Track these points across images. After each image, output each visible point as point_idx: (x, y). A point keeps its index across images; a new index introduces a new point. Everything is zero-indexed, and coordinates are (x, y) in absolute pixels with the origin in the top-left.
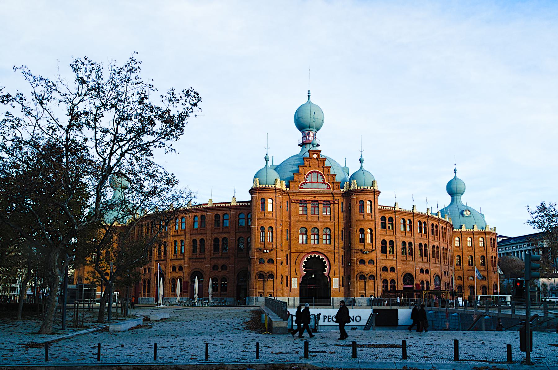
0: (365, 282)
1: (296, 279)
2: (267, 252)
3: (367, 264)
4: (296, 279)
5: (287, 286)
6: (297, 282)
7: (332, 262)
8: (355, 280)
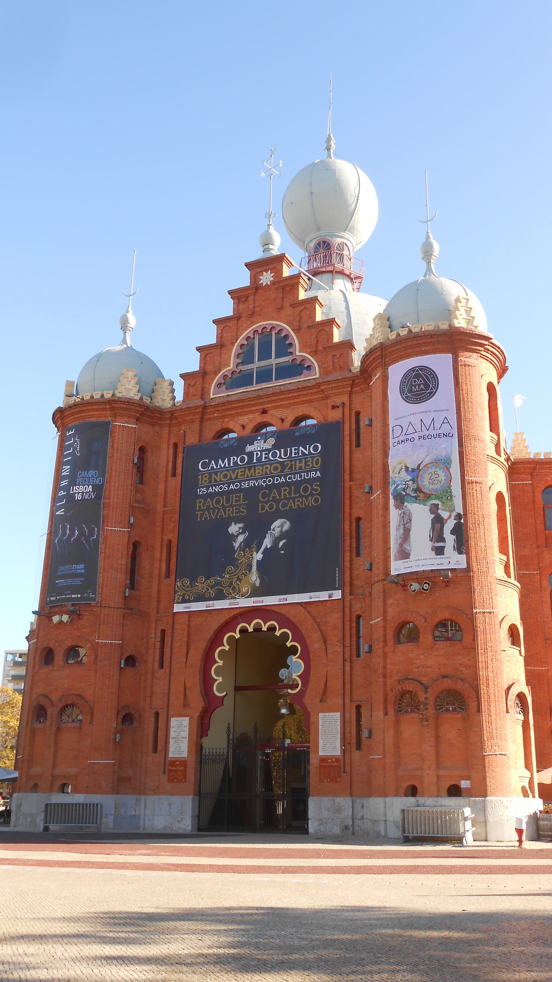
0: (422, 720)
1: (185, 721)
2: (61, 622)
3: (426, 638)
4: (185, 721)
5: (155, 750)
6: (185, 733)
7: (316, 646)
8: (381, 714)
